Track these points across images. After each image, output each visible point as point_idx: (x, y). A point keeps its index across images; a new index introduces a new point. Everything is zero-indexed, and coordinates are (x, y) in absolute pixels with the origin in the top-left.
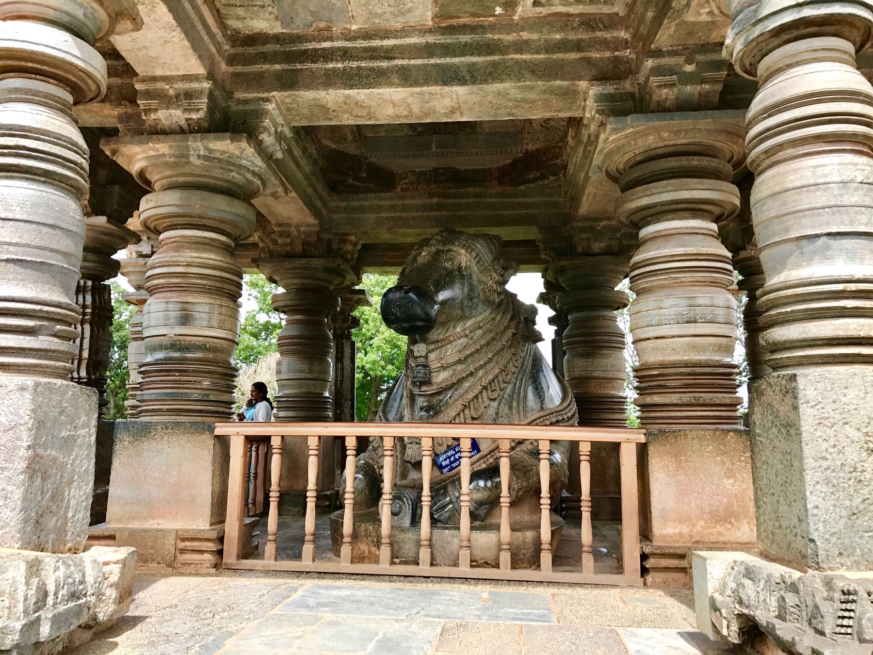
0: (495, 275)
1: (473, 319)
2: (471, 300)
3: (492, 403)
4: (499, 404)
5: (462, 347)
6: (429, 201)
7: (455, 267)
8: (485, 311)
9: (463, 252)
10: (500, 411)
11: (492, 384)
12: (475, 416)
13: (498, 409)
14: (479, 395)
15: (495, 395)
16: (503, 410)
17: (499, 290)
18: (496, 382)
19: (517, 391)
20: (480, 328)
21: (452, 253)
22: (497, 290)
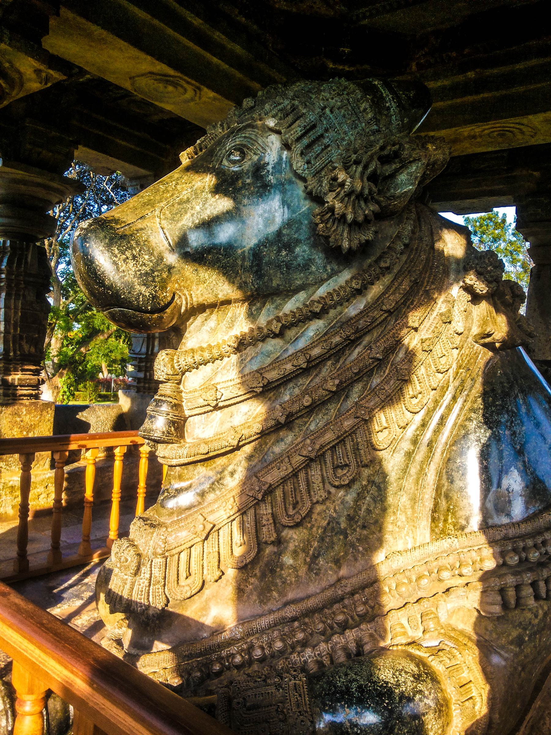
0: (342, 176)
1: (302, 296)
2: (289, 246)
3: (341, 493)
4: (360, 497)
5: (269, 361)
6: (460, 78)
7: (247, 165)
8: (334, 273)
9: (271, 123)
10: (362, 513)
11: (340, 451)
12: (285, 521)
13: (357, 507)
14: (302, 475)
15: (345, 476)
16: (369, 511)
17: (350, 217)
18: (349, 445)
19: (414, 470)
20: (316, 316)
21: (248, 133)
22: (344, 216)
